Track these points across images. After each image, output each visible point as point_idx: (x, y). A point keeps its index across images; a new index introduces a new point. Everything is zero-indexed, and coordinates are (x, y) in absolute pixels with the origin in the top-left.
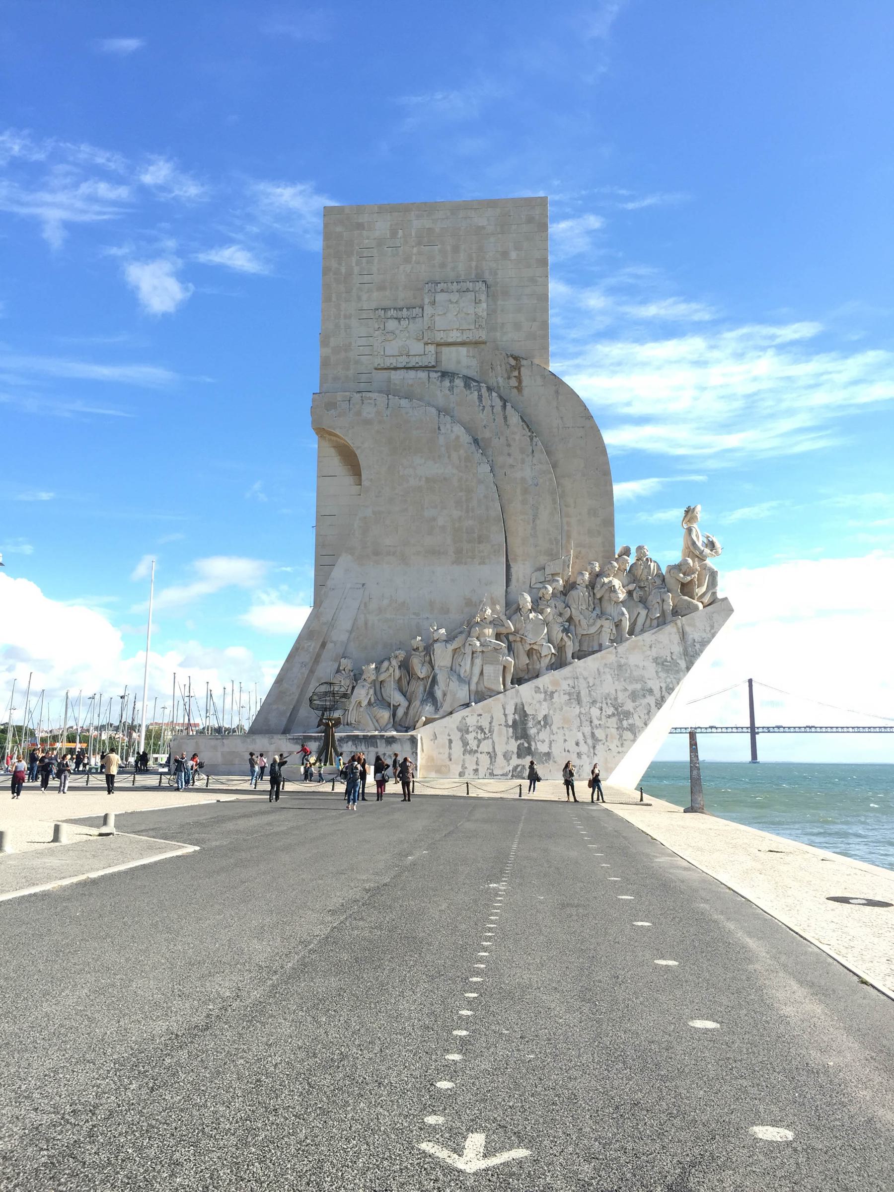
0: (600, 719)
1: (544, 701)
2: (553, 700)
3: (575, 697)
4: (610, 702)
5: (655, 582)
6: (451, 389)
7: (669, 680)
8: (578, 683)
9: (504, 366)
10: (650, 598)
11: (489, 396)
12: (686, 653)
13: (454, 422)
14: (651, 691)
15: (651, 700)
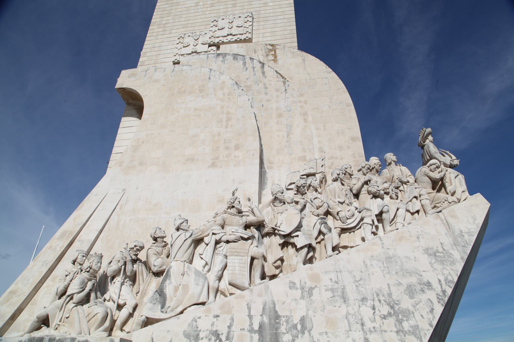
0: (374, 321)
1: (301, 298)
2: (312, 298)
3: (340, 293)
4: (383, 298)
5: (408, 182)
6: (223, 61)
7: (446, 272)
8: (341, 277)
9: (264, 51)
10: (407, 195)
11: (251, 62)
12: (456, 244)
13: (222, 74)
14: (429, 284)
15: (431, 295)
